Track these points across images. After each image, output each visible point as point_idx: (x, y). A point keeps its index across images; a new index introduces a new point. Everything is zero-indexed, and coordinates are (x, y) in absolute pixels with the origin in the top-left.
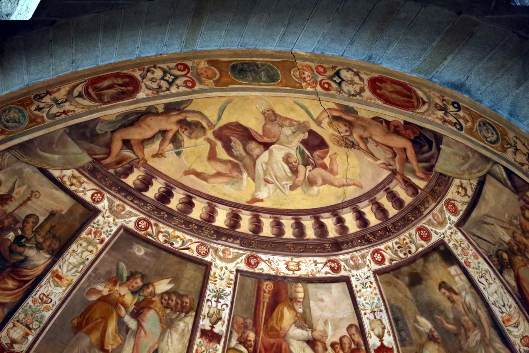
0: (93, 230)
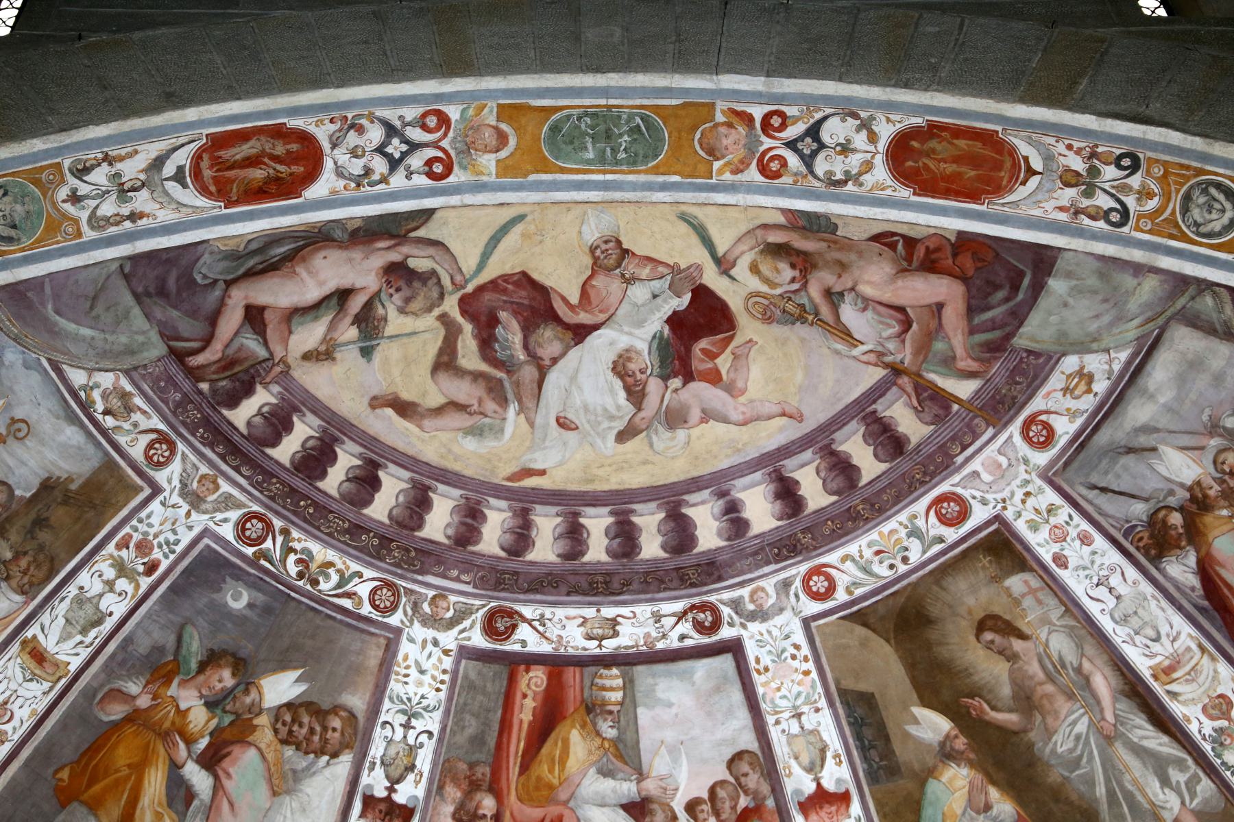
0: (137, 537)
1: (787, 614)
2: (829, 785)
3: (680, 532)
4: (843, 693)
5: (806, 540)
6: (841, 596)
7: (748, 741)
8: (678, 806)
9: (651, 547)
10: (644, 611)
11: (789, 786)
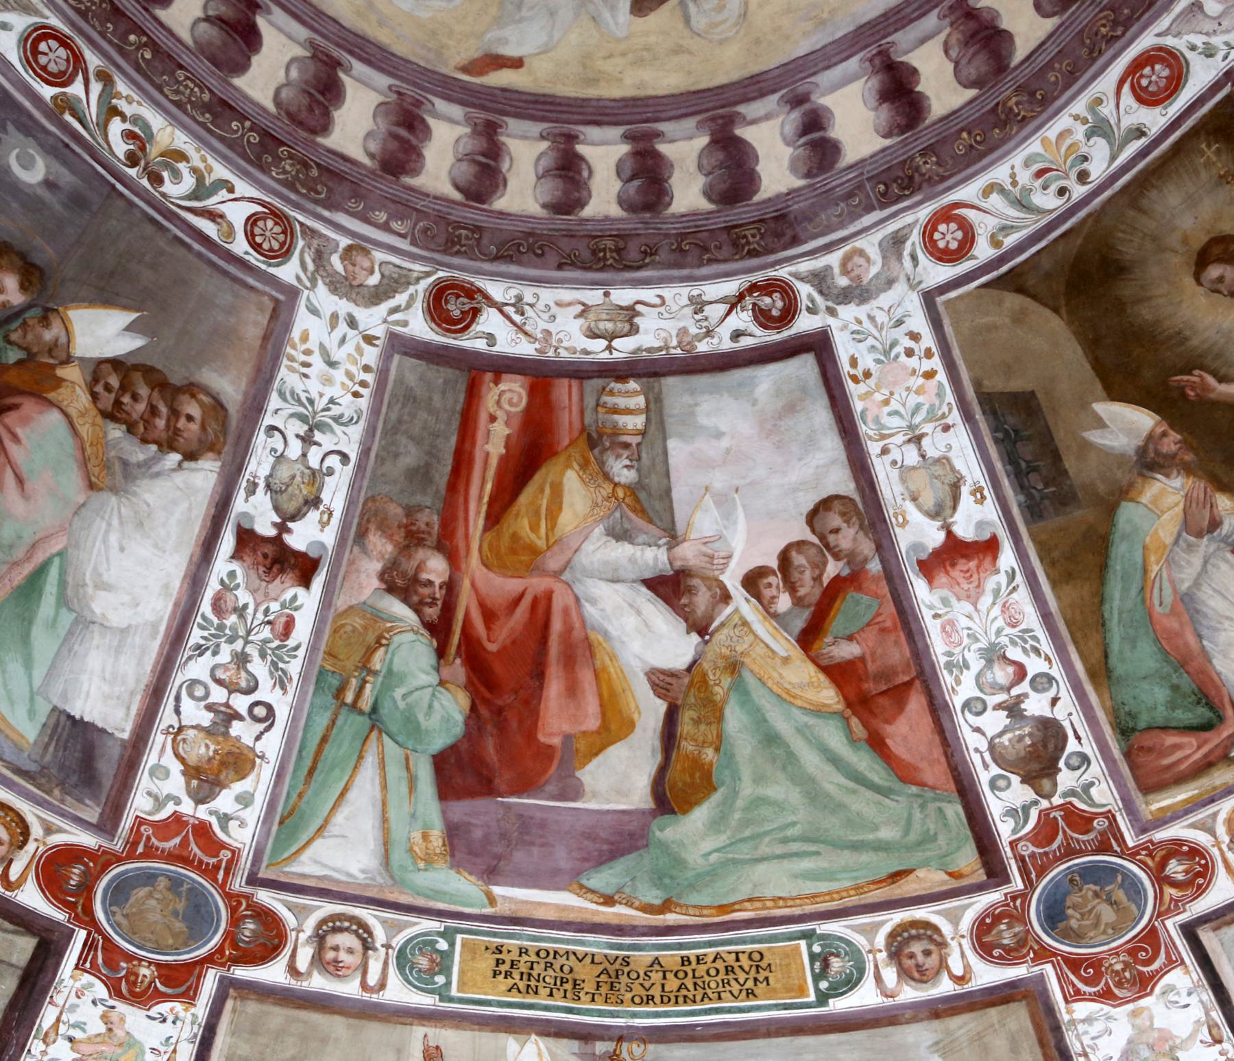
1: (900, 288)
2: (965, 529)
3: (733, 168)
4: (986, 399)
5: (929, 166)
6: (983, 251)
7: (841, 482)
8: (732, 579)
9: (688, 194)
10: (678, 294)
11: (904, 539)
